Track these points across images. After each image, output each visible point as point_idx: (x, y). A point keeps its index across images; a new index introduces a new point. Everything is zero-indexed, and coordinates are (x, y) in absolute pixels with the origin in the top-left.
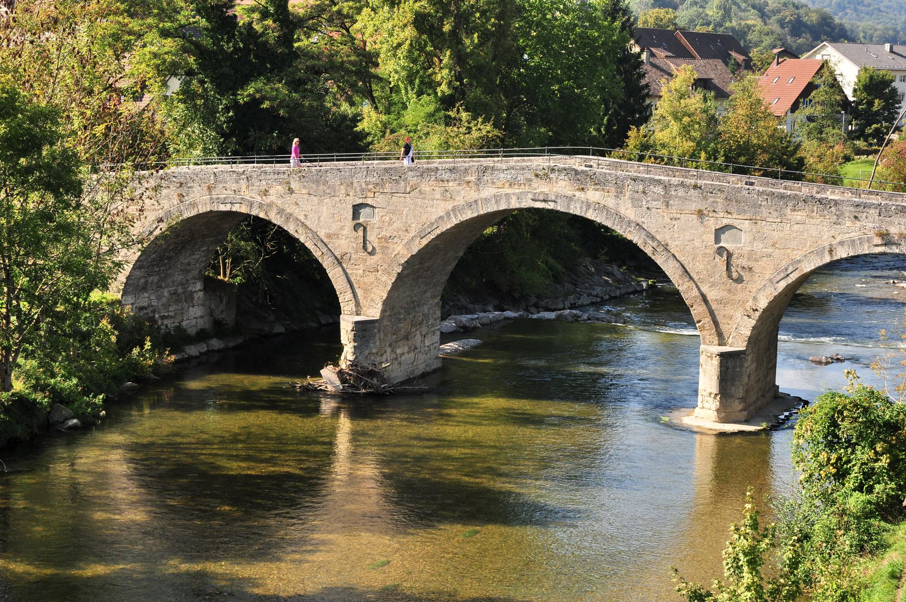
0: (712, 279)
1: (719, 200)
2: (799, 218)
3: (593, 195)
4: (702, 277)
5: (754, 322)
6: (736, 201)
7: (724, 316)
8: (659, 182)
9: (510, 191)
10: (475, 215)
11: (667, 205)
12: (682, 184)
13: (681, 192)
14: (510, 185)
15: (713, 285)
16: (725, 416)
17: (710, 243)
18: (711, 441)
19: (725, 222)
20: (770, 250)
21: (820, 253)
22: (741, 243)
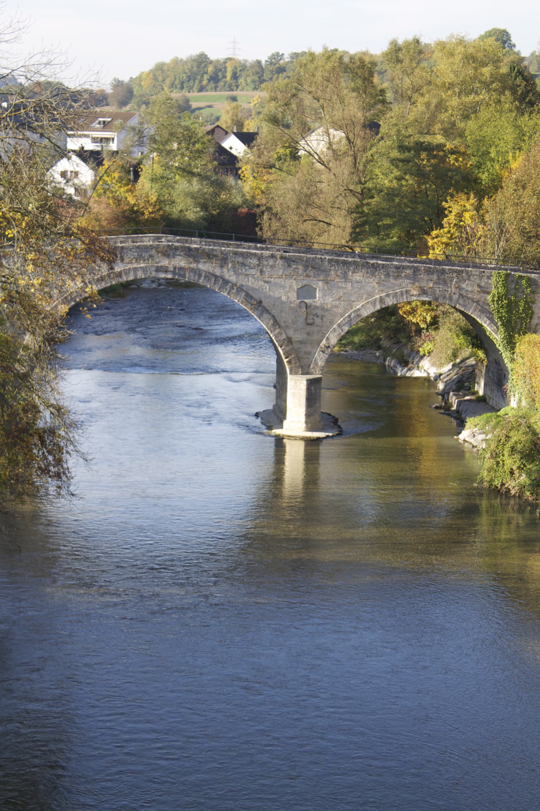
0: (295, 326)
1: (300, 267)
2: (358, 278)
3: (204, 266)
4: (287, 324)
5: (327, 356)
6: (312, 267)
7: (305, 353)
8: (255, 255)
9: (135, 266)
10: (109, 285)
11: (262, 272)
12: (272, 256)
13: (271, 262)
14: (136, 260)
15: (296, 330)
16: (310, 427)
17: (293, 299)
18: (301, 445)
19: (305, 282)
20: (337, 303)
21: (374, 303)
22: (315, 298)
